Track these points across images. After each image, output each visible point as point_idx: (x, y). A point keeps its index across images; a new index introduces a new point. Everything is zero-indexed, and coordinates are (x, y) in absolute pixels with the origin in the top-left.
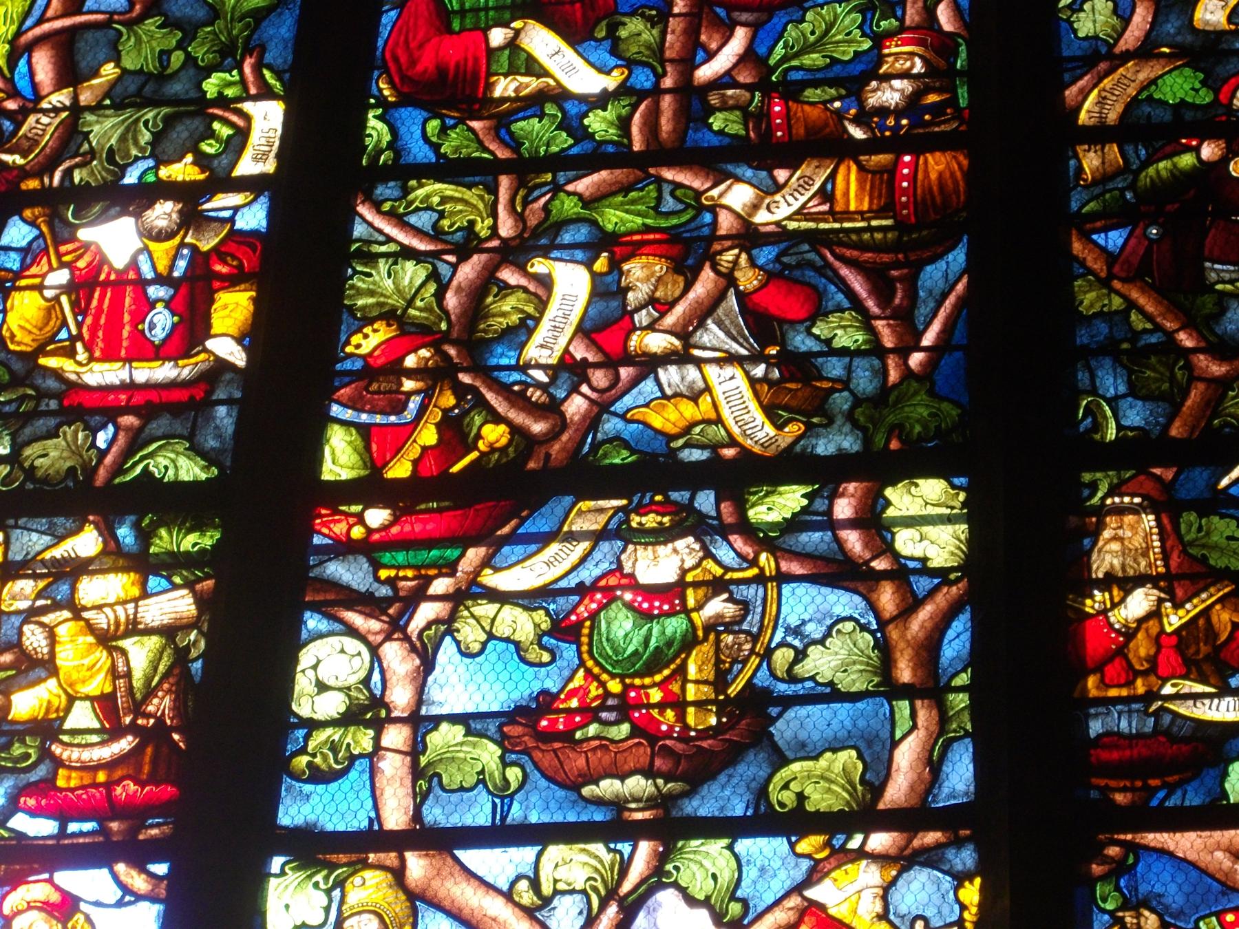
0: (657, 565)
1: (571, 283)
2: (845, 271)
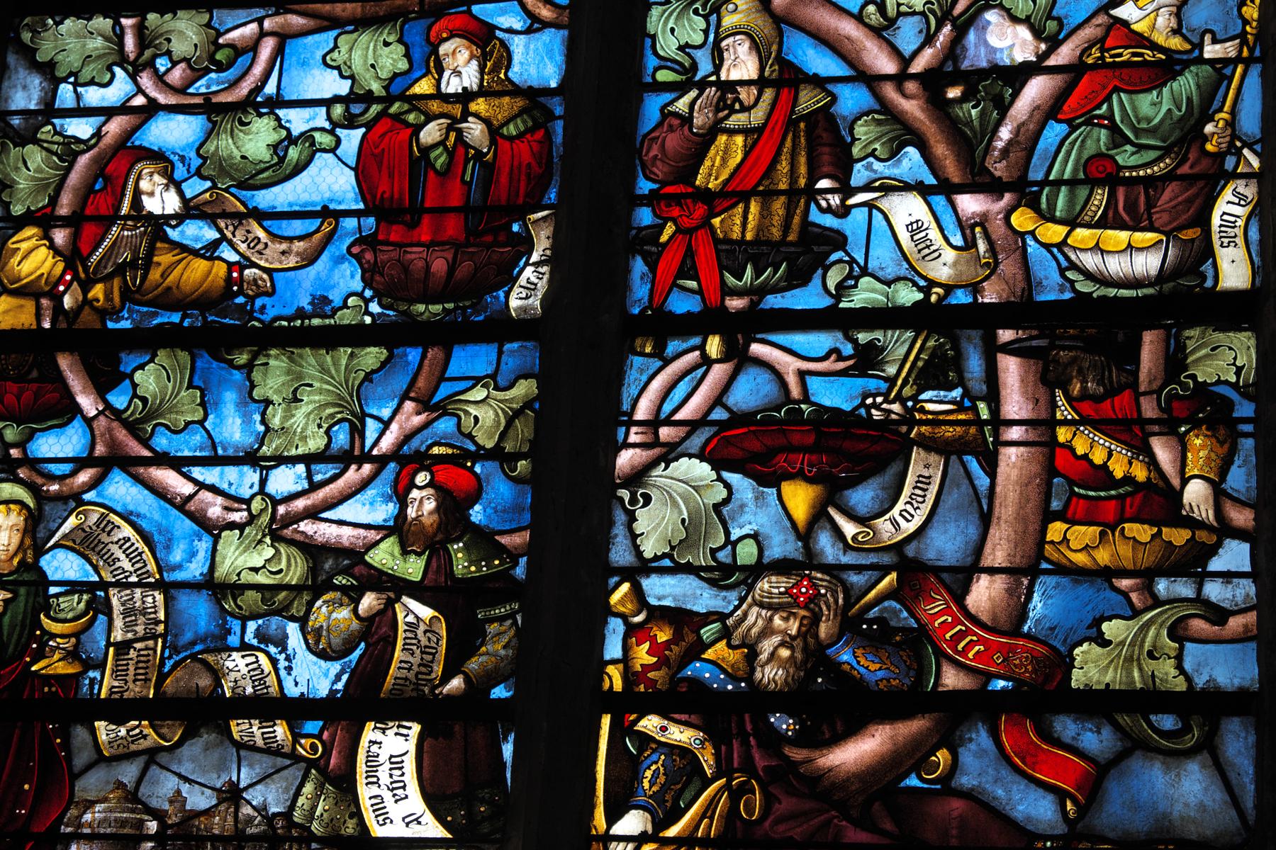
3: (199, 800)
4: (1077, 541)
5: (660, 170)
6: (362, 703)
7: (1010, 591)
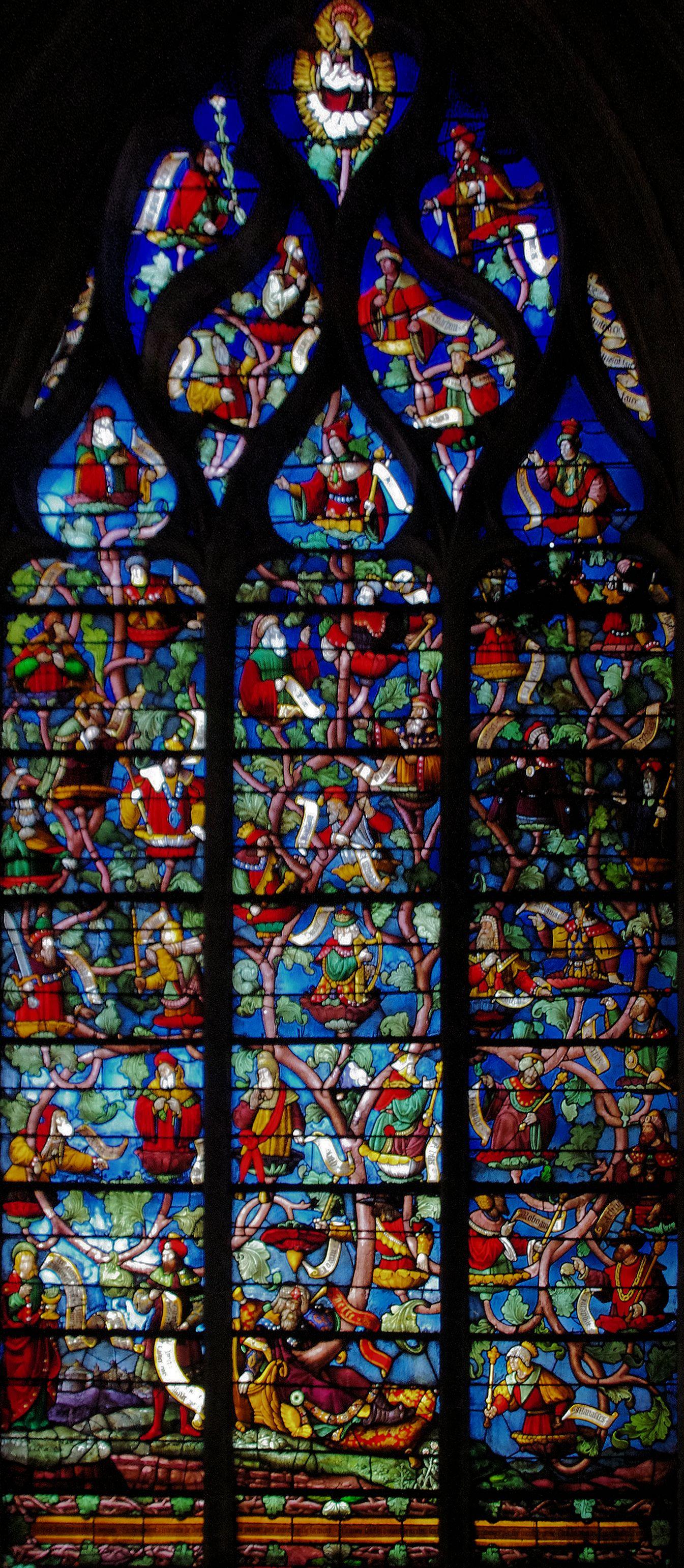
0: (345, 938)
1: (311, 809)
2: (402, 811)
3: (104, 1367)
4: (383, 1276)
5: (240, 1124)
6: (153, 1332)
7: (364, 1294)
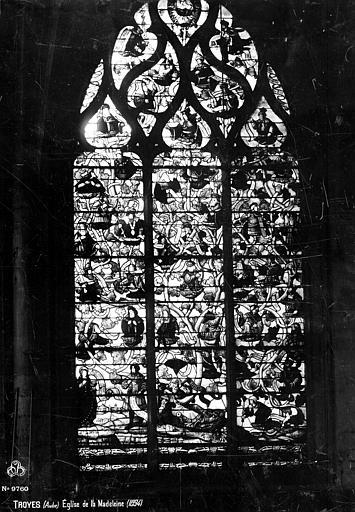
0: (191, 269)
